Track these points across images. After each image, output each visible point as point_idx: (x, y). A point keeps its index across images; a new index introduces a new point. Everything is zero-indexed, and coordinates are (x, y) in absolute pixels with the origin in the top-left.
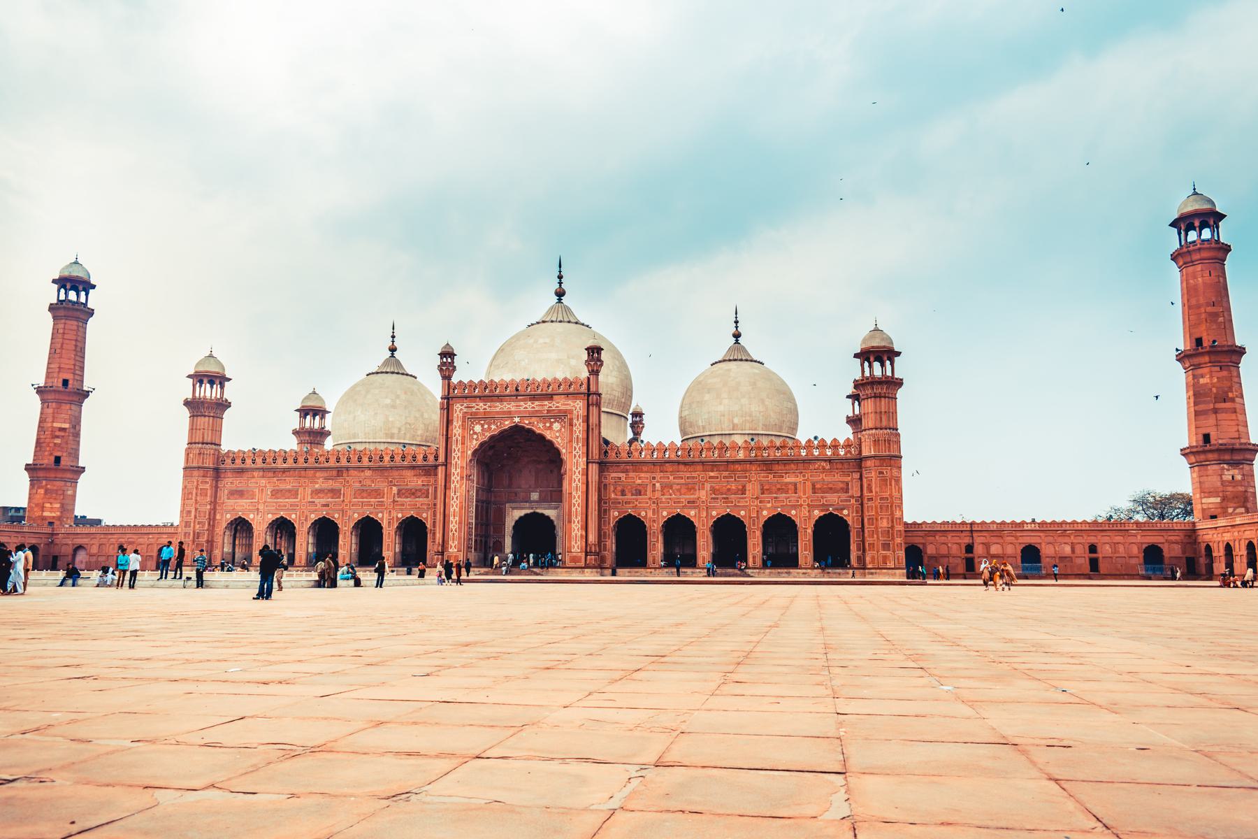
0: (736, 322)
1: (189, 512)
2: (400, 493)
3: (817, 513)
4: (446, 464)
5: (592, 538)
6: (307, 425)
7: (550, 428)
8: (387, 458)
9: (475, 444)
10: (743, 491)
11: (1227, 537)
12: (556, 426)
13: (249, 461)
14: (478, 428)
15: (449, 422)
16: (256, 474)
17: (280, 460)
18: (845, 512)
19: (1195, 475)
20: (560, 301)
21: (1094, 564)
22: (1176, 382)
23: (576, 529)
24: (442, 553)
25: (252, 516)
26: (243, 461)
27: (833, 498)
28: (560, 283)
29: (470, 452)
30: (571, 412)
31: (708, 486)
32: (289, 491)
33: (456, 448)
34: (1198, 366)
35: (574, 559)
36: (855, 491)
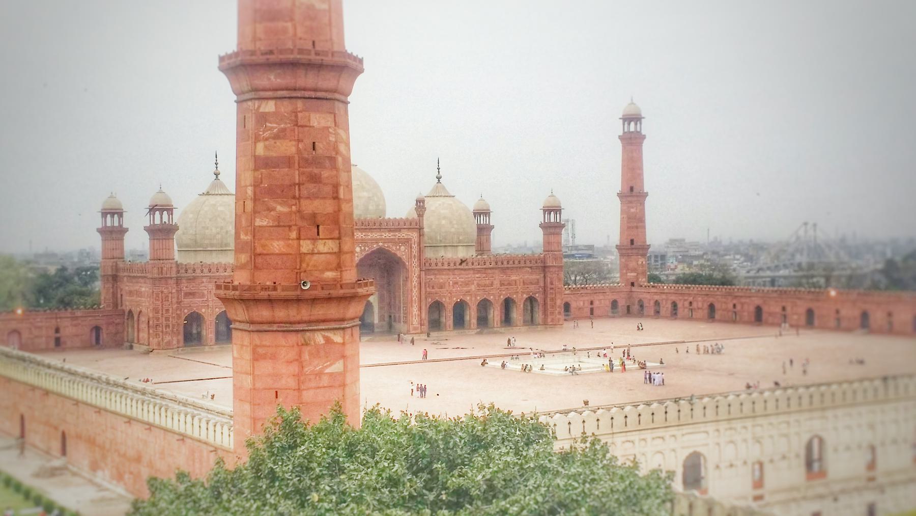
1: (167, 311)
3: (525, 296)
5: (423, 316)
6: (109, 224)
7: (399, 249)
10: (492, 284)
12: (403, 248)
13: (198, 271)
16: (204, 280)
17: (221, 270)
19: (623, 260)
21: (592, 313)
22: (615, 207)
25: (203, 310)
26: (194, 271)
27: (532, 288)
30: (410, 240)
31: (475, 282)
34: (631, 202)
35: (415, 329)
36: (542, 284)
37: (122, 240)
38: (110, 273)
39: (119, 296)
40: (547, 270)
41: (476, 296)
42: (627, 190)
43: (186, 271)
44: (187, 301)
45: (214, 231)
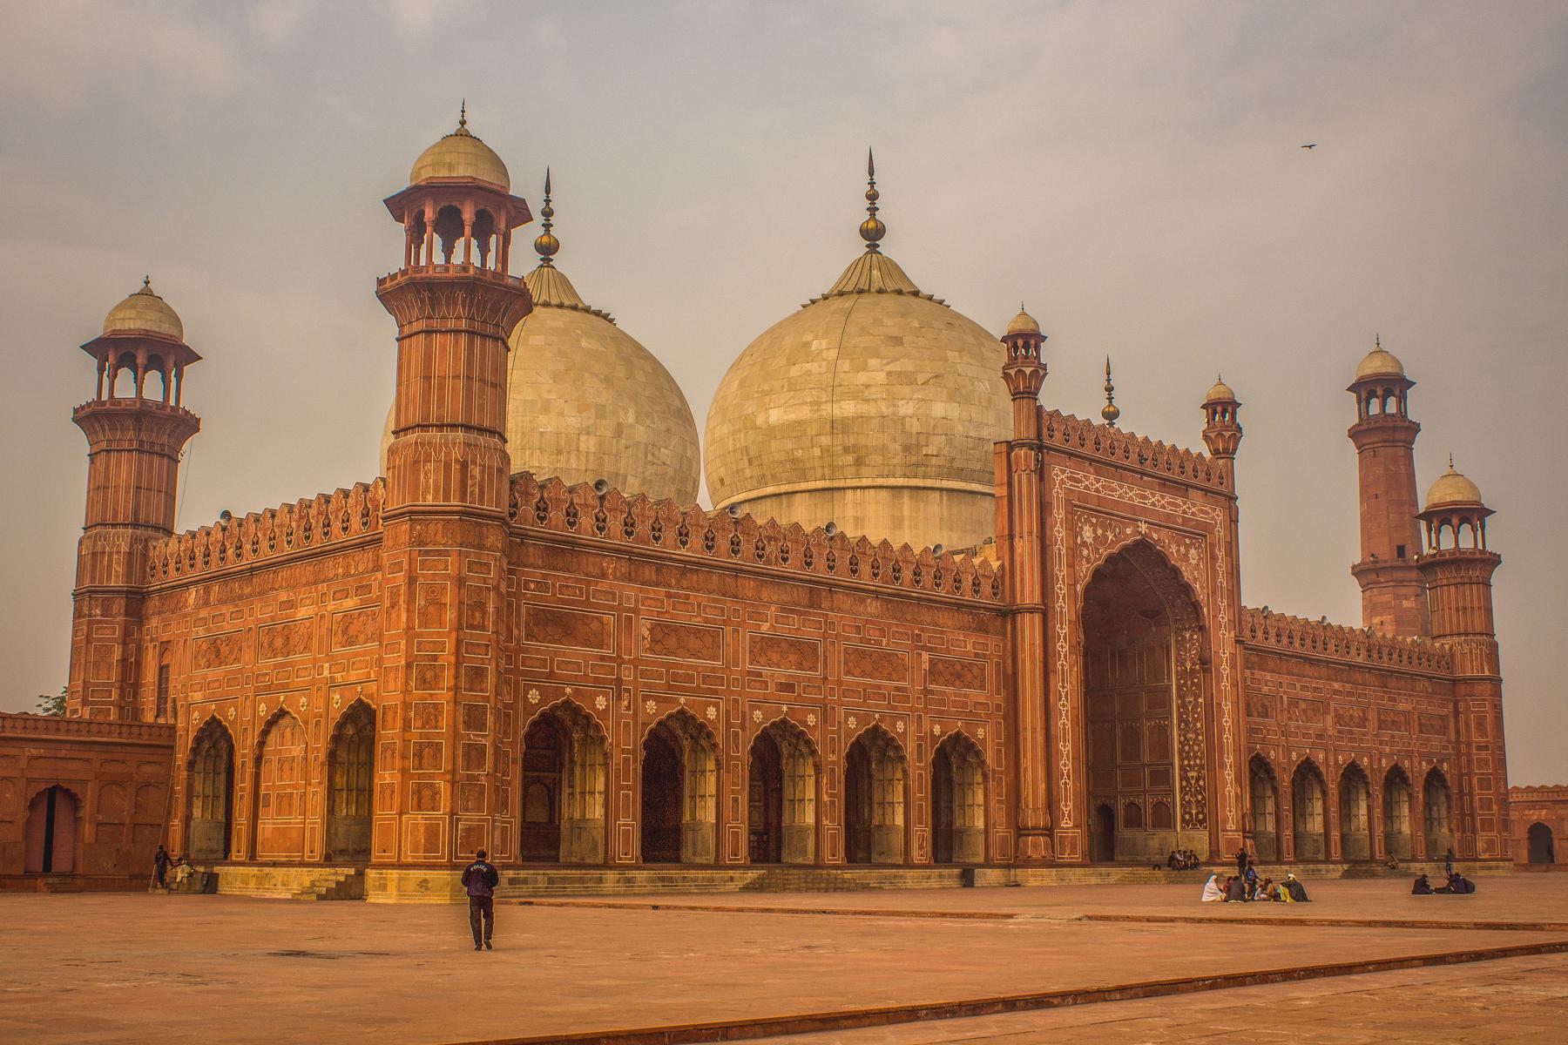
0: (1109, 389)
1: (478, 674)
2: (933, 674)
4: (1045, 612)
7: (1186, 555)
8: (907, 574)
9: (1085, 570)
10: (1364, 719)
11: (1536, 815)
13: (586, 521)
14: (1088, 534)
15: (1044, 508)
17: (670, 535)
18: (1445, 765)
20: (873, 248)
23: (1229, 775)
24: (1049, 831)
26: (572, 515)
27: (1436, 742)
28: (873, 210)
29: (1079, 588)
32: (698, 633)
33: (1061, 572)
34: (1401, 583)
37: (172, 458)
38: (116, 582)
39: (150, 676)
40: (1462, 689)
41: (1336, 751)
42: (1386, 552)
43: (542, 508)
44: (539, 648)
45: (573, 421)
